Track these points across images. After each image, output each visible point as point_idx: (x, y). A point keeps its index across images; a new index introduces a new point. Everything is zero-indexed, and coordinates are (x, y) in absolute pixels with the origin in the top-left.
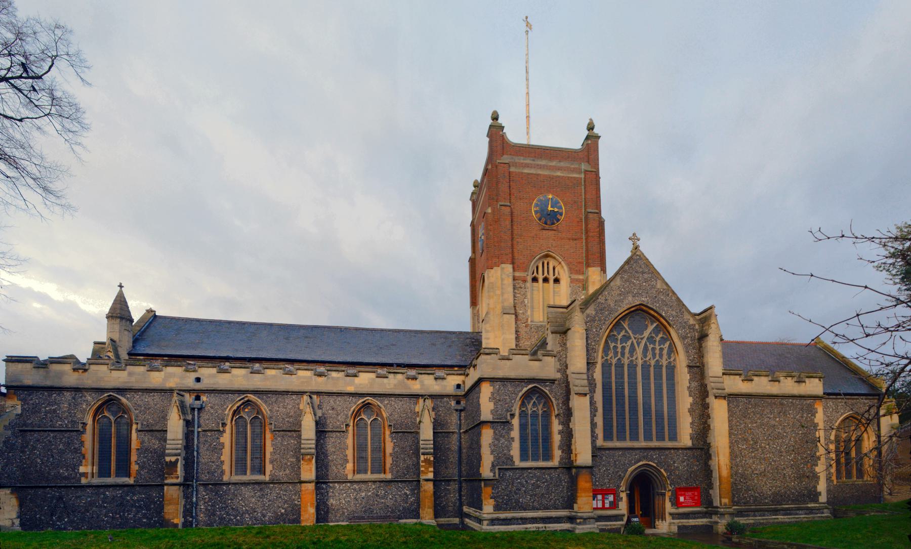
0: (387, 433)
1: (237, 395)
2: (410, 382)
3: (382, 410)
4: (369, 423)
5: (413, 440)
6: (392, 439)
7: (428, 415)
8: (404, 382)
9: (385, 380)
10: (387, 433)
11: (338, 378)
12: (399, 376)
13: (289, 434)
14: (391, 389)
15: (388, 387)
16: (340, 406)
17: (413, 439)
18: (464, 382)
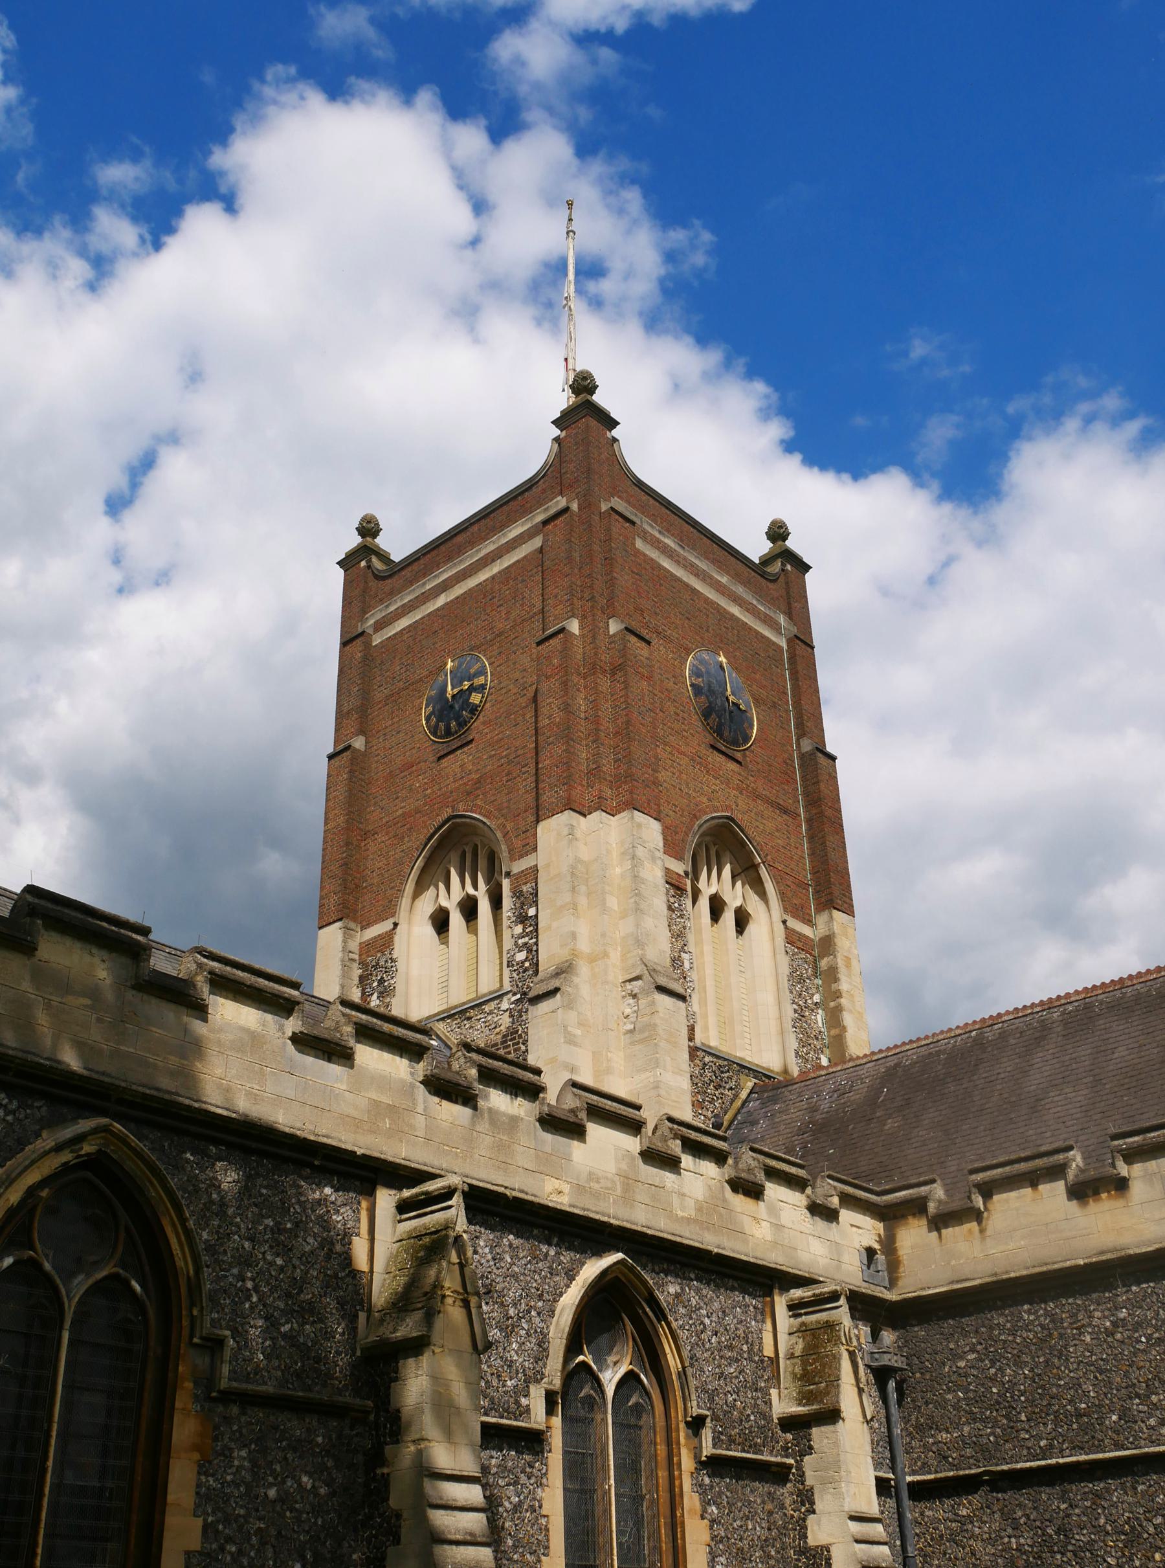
0: (687, 1462)
1: (41, 1108)
2: (739, 1202)
3: (662, 1330)
4: (610, 1390)
5: (770, 1513)
6: (705, 1503)
7: (853, 1381)
8: (725, 1200)
9: (668, 1177)
10: (687, 1462)
11: (514, 1120)
12: (709, 1168)
13: (296, 1427)
14: (689, 1220)
15: (680, 1213)
16: (514, 1276)
17: (769, 1506)
18: (889, 1243)
